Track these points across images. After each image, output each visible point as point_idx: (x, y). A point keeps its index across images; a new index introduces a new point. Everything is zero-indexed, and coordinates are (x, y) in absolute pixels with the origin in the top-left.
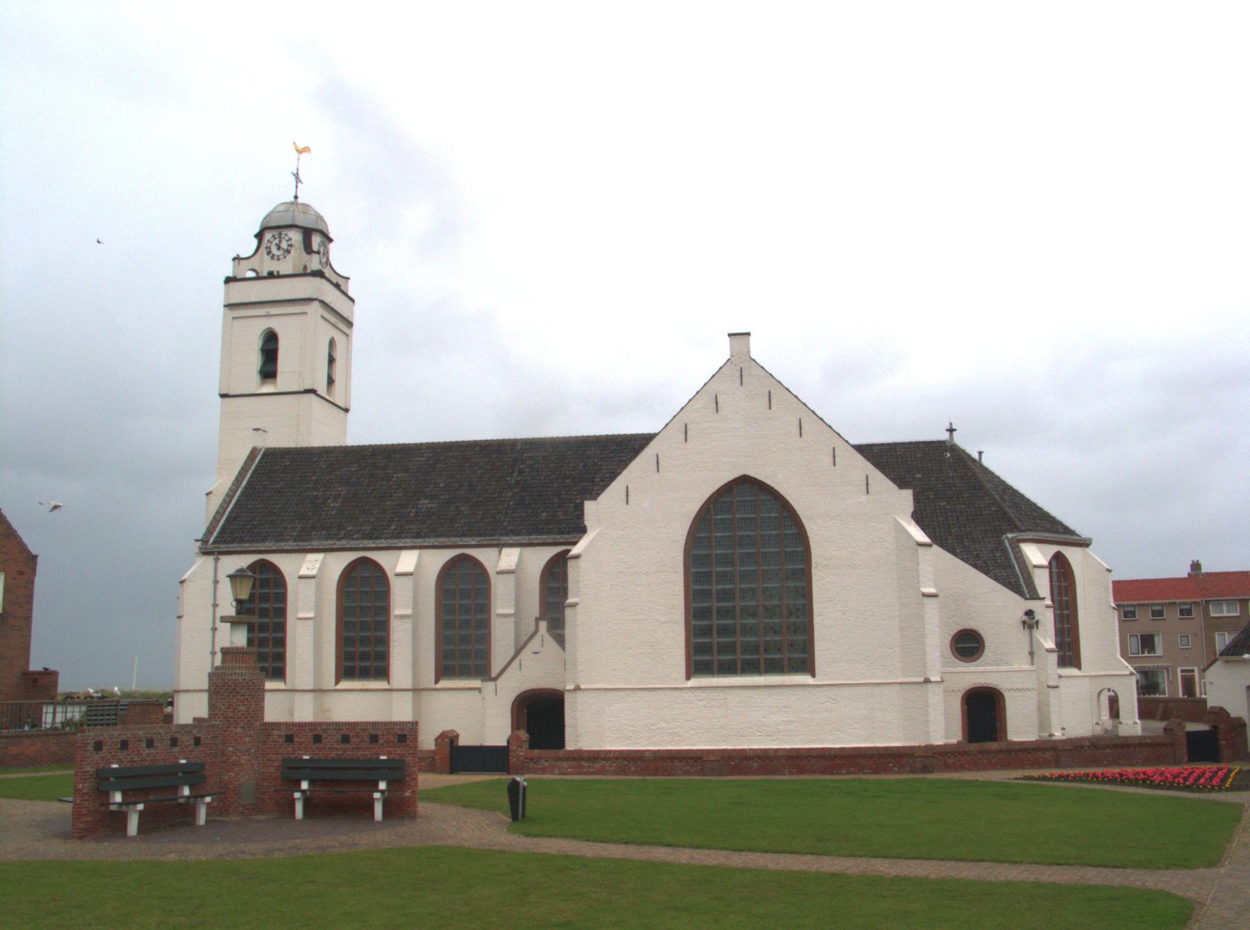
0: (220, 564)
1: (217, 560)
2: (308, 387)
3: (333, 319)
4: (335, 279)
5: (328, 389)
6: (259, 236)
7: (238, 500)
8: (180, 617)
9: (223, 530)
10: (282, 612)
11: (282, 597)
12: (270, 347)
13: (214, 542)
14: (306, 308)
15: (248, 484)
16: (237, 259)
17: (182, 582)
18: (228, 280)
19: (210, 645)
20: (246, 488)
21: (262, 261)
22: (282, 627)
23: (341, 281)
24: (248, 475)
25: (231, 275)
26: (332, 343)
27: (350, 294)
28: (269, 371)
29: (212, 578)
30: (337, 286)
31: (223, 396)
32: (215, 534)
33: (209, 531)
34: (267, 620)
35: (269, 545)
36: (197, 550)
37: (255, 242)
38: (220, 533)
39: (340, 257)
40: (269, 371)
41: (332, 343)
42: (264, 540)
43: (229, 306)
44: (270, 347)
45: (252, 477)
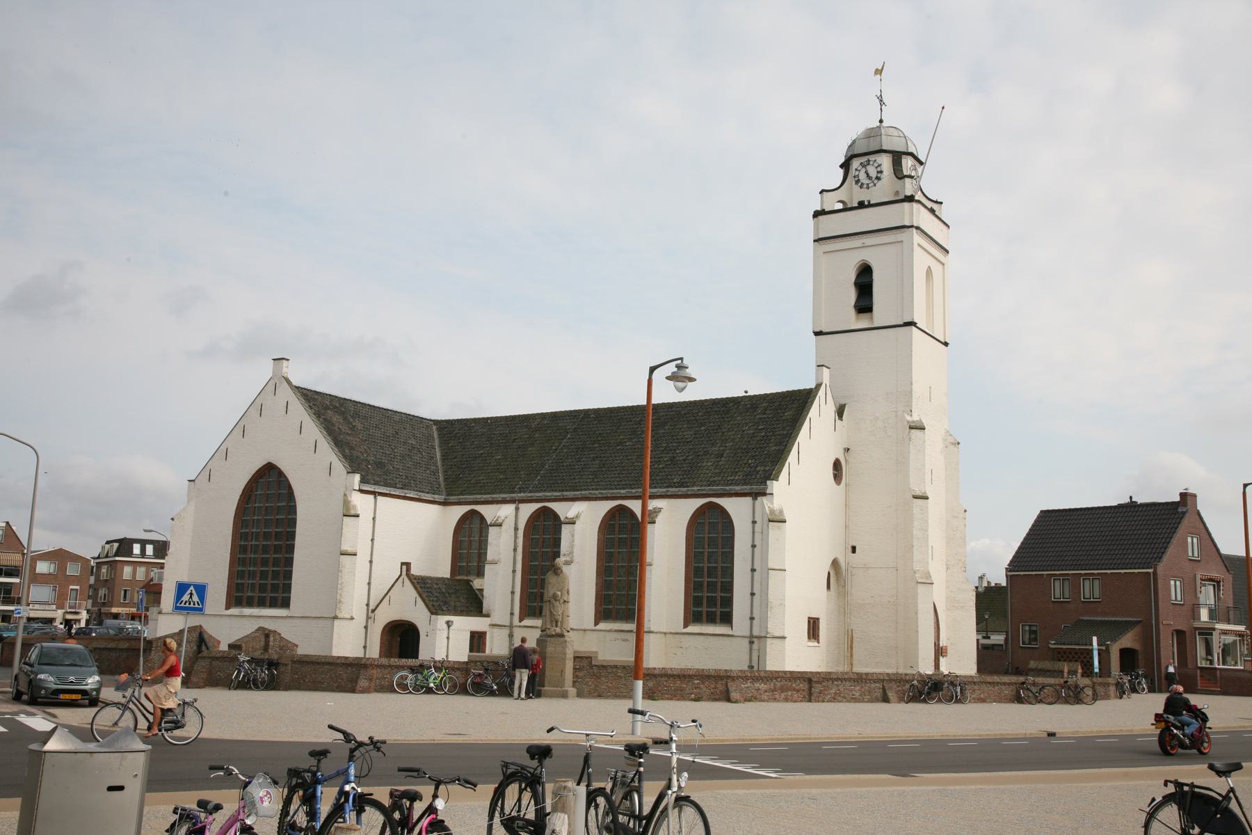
4: (930, 204)
12: (864, 282)
23: (935, 206)
26: (929, 272)
28: (864, 305)
30: (932, 211)
31: (817, 334)
39: (931, 182)
40: (864, 305)
41: (929, 272)
44: (864, 282)
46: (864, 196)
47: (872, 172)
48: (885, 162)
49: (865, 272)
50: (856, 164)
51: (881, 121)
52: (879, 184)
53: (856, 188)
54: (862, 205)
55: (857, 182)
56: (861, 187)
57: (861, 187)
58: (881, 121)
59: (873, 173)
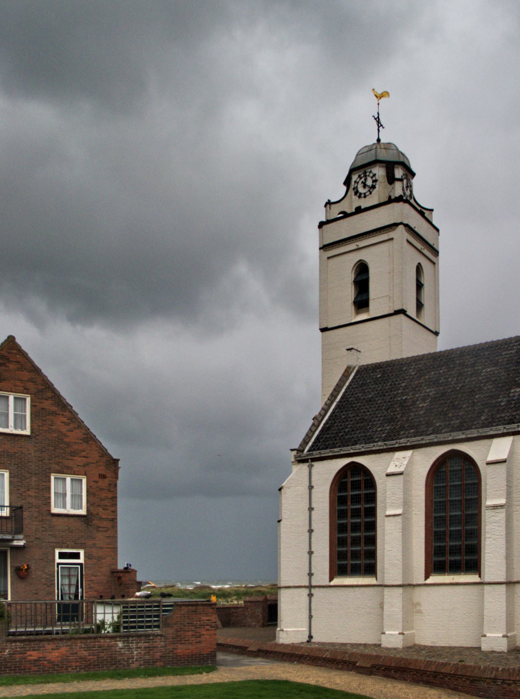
0: (314, 470)
1: (310, 467)
2: (397, 308)
3: (419, 246)
4: (419, 209)
5: (418, 308)
6: (347, 182)
7: (333, 412)
8: (279, 521)
9: (318, 438)
10: (372, 512)
11: (372, 498)
13: (309, 451)
14: (391, 234)
15: (342, 398)
16: (329, 203)
17: (280, 489)
18: (321, 225)
19: (308, 547)
20: (340, 401)
21: (351, 203)
22: (372, 526)
24: (343, 390)
25: (324, 220)
27: (434, 223)
29: (307, 484)
30: (422, 214)
32: (310, 444)
33: (305, 442)
34: (359, 520)
35: (359, 448)
36: (293, 459)
37: (345, 188)
38: (315, 442)
42: (355, 443)
43: (324, 248)
45: (346, 391)
46: (364, 203)
47: (369, 182)
48: (379, 172)
49: (362, 269)
50: (355, 177)
51: (379, 140)
52: (374, 192)
53: (355, 198)
54: (359, 210)
55: (356, 193)
56: (360, 197)
57: (360, 197)
58: (379, 140)
59: (369, 182)
